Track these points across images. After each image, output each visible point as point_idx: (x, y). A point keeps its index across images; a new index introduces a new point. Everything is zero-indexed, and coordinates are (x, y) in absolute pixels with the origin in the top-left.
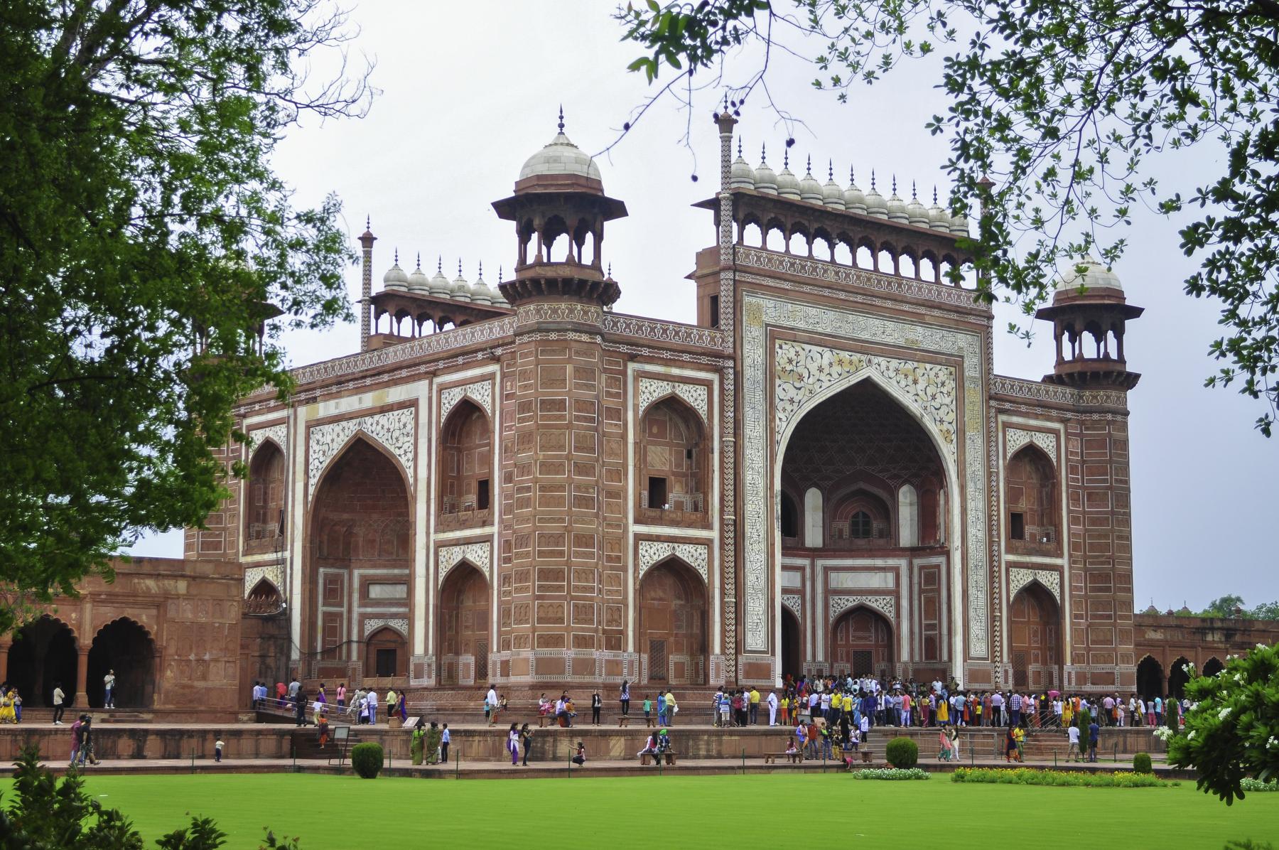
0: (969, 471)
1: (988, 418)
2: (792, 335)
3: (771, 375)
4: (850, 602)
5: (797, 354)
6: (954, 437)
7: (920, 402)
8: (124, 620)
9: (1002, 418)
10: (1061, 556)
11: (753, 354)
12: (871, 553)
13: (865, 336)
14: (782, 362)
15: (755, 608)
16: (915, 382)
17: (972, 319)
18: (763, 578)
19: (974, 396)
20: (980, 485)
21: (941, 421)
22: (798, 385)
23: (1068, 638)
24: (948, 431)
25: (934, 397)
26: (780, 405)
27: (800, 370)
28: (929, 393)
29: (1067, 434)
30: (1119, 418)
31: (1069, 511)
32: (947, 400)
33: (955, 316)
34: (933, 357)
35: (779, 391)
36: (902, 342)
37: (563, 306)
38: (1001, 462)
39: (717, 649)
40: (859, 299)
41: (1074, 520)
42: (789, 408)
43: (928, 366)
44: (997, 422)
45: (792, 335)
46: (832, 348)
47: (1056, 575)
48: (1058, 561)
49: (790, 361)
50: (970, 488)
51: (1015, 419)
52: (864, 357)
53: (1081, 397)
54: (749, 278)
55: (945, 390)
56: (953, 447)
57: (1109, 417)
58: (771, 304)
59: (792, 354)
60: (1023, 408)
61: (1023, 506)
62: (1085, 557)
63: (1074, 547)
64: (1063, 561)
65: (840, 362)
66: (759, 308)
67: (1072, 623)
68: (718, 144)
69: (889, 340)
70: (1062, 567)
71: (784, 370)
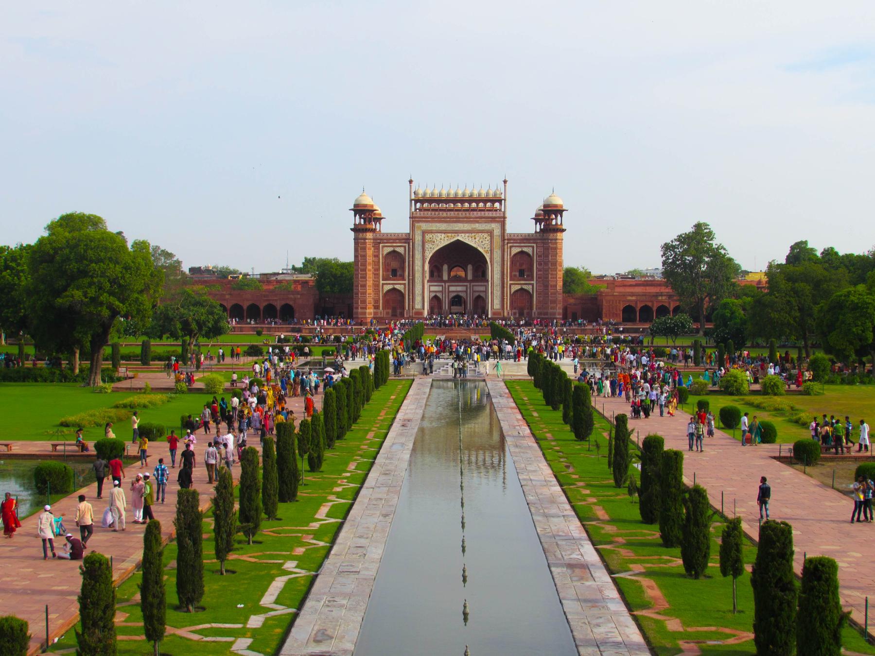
1: (503, 246)
2: (431, 232)
4: (477, 294)
11: (418, 238)
12: (482, 281)
15: (418, 299)
18: (421, 292)
19: (497, 240)
34: (482, 232)
41: (538, 270)
45: (431, 232)
47: (531, 287)
50: (495, 265)
61: (524, 267)
63: (538, 278)
64: (534, 282)
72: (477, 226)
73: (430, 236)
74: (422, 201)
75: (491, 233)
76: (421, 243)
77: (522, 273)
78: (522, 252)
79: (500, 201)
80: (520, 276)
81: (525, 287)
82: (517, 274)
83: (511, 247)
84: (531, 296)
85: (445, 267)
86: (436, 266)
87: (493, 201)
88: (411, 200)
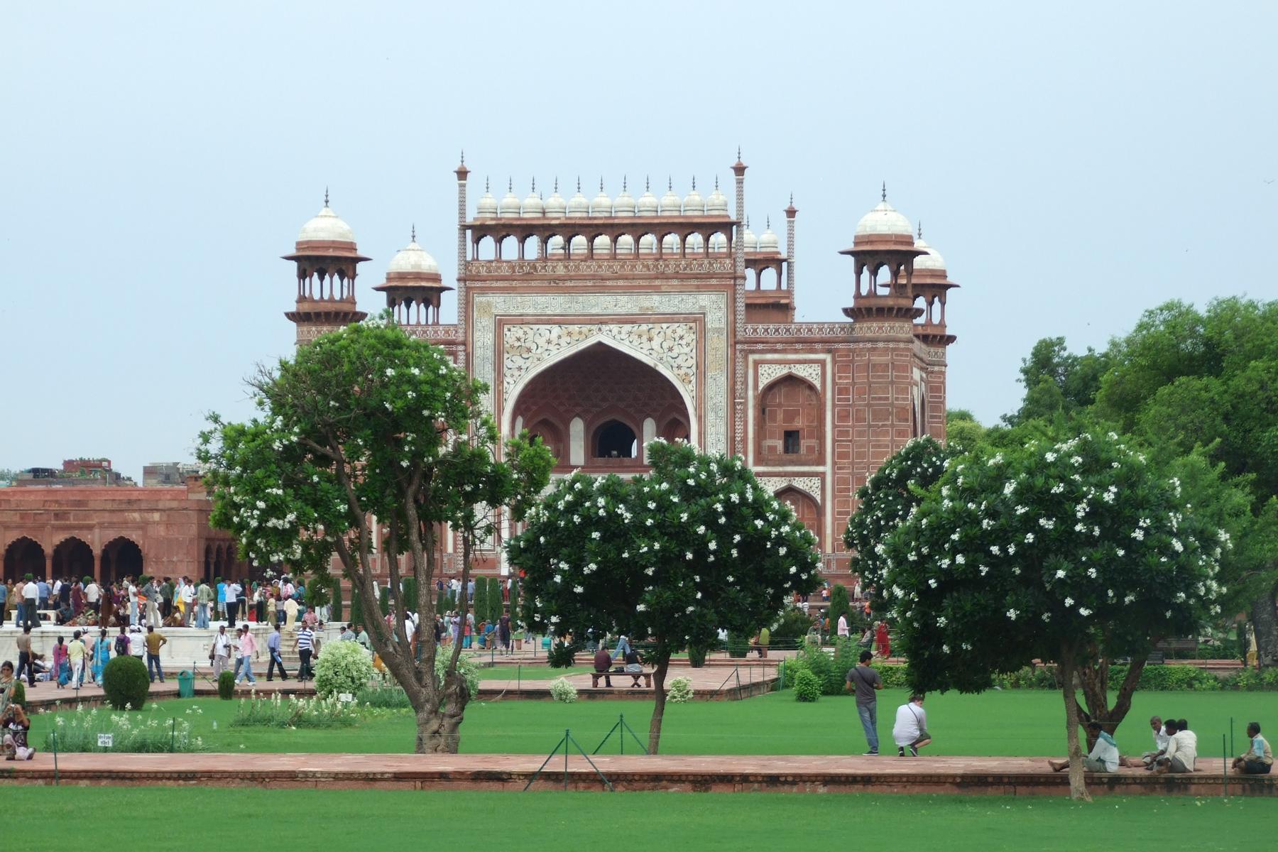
0: (709, 404)
2: (521, 320)
3: (499, 351)
5: (525, 333)
6: (693, 379)
7: (655, 355)
8: (122, 538)
9: (751, 358)
10: (821, 461)
11: (483, 339)
13: (593, 311)
14: (511, 341)
16: (650, 340)
17: (714, 282)
19: (718, 345)
20: (722, 413)
21: (679, 367)
22: (525, 356)
23: (829, 531)
24: (686, 374)
25: (671, 349)
26: (508, 373)
27: (527, 345)
28: (665, 345)
29: (834, 362)
30: (881, 345)
31: (834, 426)
32: (687, 350)
33: (696, 282)
34: (671, 318)
35: (507, 363)
36: (636, 310)
37: (305, 329)
38: (750, 393)
39: (450, 549)
40: (589, 284)
42: (516, 373)
43: (665, 326)
44: (746, 358)
45: (521, 320)
46: (559, 323)
48: (820, 469)
49: (519, 340)
50: (711, 417)
51: (769, 356)
52: (595, 327)
53: (853, 329)
54: (479, 284)
55: (683, 342)
56: (692, 387)
57: (869, 345)
58: (502, 299)
59: (520, 333)
60: (779, 346)
61: (799, 423)
62: (852, 463)
63: (839, 455)
64: (827, 469)
65: (569, 334)
66: (489, 304)
67: (834, 519)
68: (457, 188)
69: (623, 311)
70: (824, 473)
71: (512, 347)
72: (655, 302)
73: (517, 331)
74: (500, 230)
75: (697, 320)
76: (490, 353)
77: (791, 438)
78: (790, 381)
79: (726, 227)
80: (787, 450)
81: (799, 483)
82: (779, 444)
83: (757, 363)
84: (819, 510)
85: (577, 429)
86: (545, 423)
87: (708, 228)
88: (464, 228)
